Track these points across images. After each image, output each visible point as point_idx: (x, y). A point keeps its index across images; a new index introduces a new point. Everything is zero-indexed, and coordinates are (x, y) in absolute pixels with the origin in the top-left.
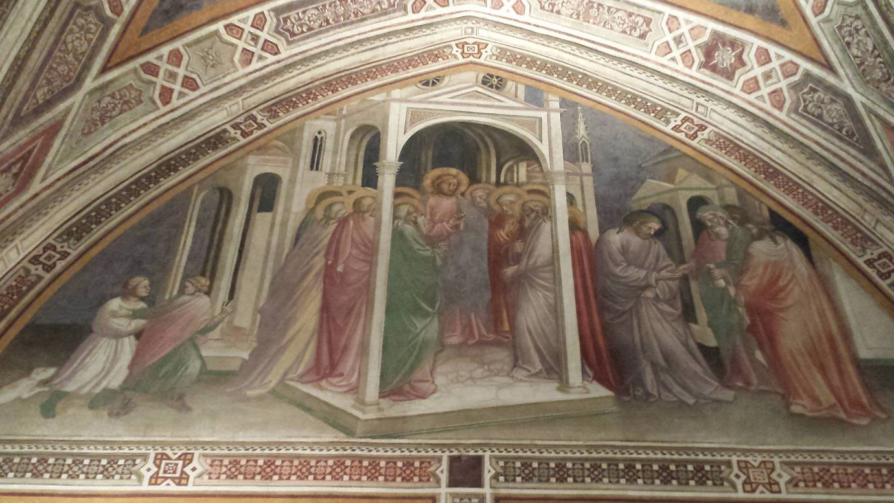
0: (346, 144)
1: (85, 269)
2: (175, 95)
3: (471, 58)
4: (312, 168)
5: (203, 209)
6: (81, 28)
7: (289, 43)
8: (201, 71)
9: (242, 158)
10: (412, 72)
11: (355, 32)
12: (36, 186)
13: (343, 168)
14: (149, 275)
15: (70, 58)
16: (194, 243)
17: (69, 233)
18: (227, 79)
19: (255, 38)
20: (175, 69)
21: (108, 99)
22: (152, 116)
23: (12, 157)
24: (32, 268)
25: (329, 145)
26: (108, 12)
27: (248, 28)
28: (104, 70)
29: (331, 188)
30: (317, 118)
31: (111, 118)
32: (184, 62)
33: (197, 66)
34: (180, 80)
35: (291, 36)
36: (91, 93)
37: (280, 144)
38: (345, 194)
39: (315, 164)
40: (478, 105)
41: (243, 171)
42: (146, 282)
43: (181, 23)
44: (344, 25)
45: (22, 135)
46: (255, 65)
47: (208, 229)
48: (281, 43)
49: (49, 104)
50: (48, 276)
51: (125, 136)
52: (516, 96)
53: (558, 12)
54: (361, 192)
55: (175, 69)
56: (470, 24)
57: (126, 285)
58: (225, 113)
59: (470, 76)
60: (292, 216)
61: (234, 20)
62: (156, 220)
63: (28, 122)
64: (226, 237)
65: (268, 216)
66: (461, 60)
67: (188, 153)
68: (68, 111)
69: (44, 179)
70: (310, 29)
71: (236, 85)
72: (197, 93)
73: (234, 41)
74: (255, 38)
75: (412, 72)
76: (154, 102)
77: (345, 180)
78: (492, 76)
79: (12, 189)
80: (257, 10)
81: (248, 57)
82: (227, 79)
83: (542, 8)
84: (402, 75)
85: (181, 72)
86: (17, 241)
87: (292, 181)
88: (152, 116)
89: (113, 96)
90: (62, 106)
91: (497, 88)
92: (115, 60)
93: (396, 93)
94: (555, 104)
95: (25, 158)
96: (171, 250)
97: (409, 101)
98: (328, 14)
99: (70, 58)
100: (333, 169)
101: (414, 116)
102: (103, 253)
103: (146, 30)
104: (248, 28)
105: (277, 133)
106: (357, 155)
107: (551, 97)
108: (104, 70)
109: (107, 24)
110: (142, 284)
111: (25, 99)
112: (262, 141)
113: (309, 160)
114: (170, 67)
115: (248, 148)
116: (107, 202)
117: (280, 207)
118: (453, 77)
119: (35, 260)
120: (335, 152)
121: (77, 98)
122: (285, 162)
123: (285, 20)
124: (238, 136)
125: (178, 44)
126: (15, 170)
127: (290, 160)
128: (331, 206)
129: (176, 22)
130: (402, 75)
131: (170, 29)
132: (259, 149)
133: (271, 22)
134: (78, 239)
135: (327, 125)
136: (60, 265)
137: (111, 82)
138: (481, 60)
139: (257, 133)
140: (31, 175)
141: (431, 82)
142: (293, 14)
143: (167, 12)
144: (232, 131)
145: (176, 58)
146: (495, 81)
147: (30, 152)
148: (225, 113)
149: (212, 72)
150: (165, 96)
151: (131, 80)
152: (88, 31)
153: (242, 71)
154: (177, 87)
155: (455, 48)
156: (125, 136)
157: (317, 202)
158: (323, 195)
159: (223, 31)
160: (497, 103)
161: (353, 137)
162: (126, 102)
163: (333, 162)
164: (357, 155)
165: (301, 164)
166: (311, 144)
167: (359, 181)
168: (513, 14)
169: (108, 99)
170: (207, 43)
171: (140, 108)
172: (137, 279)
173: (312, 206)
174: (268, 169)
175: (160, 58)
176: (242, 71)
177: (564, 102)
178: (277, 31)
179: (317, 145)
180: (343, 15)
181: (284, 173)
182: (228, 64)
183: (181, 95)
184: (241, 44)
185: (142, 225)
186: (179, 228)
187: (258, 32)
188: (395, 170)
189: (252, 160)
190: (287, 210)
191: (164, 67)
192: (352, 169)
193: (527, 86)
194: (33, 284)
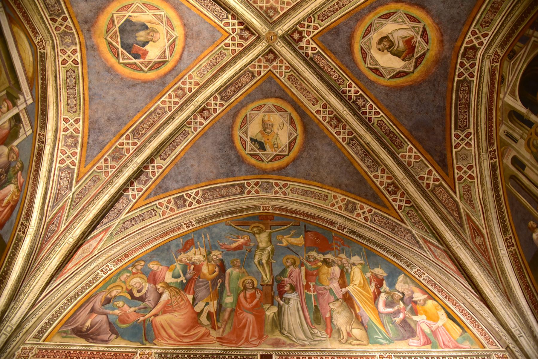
0: (512, 125)
1: (518, 236)
2: (472, 174)
3: (499, 60)
4: (516, 143)
5: (515, 188)
6: (439, 193)
7: (469, 128)
8: (468, 162)
9: (503, 163)
10: (496, 86)
11: (473, 102)
12: (484, 232)
13: (521, 131)
14: (529, 220)
15: (447, 201)
16: (525, 198)
17: (504, 232)
18: (473, 154)
19: (463, 139)
20: (463, 170)
21: (465, 196)
22: (476, 185)
23: (471, 233)
24: (510, 249)
25: (510, 131)
26: (437, 183)
27: (458, 141)
28: (455, 193)
29: (527, 140)
30: (499, 130)
31: (471, 198)
32: (462, 166)
33: (465, 163)
34: (468, 170)
35: (467, 126)
36: (461, 200)
37: (503, 148)
38: (531, 136)
39: (516, 141)
40: (518, 66)
41: (507, 166)
42: (532, 222)
43: (449, 162)
44: (469, 106)
45: (466, 226)
46: (472, 143)
47: (523, 191)
48: (468, 131)
49: (459, 213)
50: (515, 247)
51: (479, 197)
52: (521, 48)
53: (492, 20)
54: (533, 130)
55: (463, 170)
56: (486, 56)
57: (529, 228)
58: (485, 161)
59: (506, 64)
60: (531, 160)
61: (454, 144)
62: (512, 205)
63: (463, 222)
64: (528, 187)
65: (527, 168)
66: (499, 64)
67: (494, 180)
68: (464, 209)
69: (483, 228)
70: (466, 119)
71: (477, 152)
72: (474, 167)
73: (461, 147)
74: (463, 139)
75: (496, 86)
76: (472, 182)
77: (526, 133)
78: (509, 54)
79: (482, 239)
80: (453, 136)
81: (469, 144)
82: (473, 154)
83: (488, 26)
84: (496, 90)
85: (465, 169)
86: (499, 249)
87: (518, 152)
88: (476, 185)
89: (464, 194)
90: (462, 210)
91: (515, 54)
92: (453, 188)
93: (502, 96)
94: (531, 31)
95: (474, 229)
96: (525, 207)
97: (506, 93)
98: (463, 111)
99: (447, 201)
100: (520, 135)
101: (512, 94)
102: (515, 227)
103: (447, 174)
104: (458, 141)
105: (499, 148)
106: (519, 124)
107: (527, 32)
108: (455, 193)
109: (441, 185)
110: (531, 223)
111: (455, 219)
112: (500, 153)
113: (513, 142)
114: (462, 172)
115: (500, 159)
116: (500, 214)
117: (526, 162)
118: (504, 70)
119: (508, 247)
120: (514, 131)
121: (461, 205)
122: (510, 150)
123: (460, 127)
124: (495, 160)
125: (455, 166)
126: (476, 234)
127: (510, 148)
128: (533, 145)
129: (448, 163)
130: (496, 90)
131: (449, 166)
132: (502, 156)
133: (459, 132)
134: (508, 231)
135: (503, 128)
136: (513, 241)
137: (460, 192)
138: (502, 56)
139: (496, 153)
140: (480, 231)
141: (502, 80)
142: (458, 124)
143: (444, 165)
144: (492, 161)
145: (460, 169)
146: (511, 54)
147: (473, 227)
148: (485, 161)
149: (469, 159)
150: (471, 177)
151: (461, 186)
152: (441, 192)
153: (473, 148)
154: (470, 172)
155: (493, 64)
156: (479, 197)
157: (530, 148)
158: (528, 144)
159: (456, 150)
160: (521, 57)
161: (511, 121)
162: (468, 191)
163: (517, 133)
164: (519, 124)
165: (513, 145)
166: (507, 137)
167: (529, 129)
168: (487, 38)
169: (465, 196)
170: (459, 157)
171: (472, 188)
172: (529, 223)
173: (530, 151)
174: (510, 158)
175: (458, 174)
176: (473, 148)
177: (531, 27)
178: (463, 131)
179: (508, 135)
180: (465, 105)
181: (514, 153)
182: (468, 152)
183: (473, 172)
184: (463, 145)
185: (512, 210)
186: (518, 200)
187: (461, 138)
188: (530, 113)
189: (505, 161)
190: (528, 161)
191: (461, 173)
192: (523, 129)
193: (519, 41)
194: (516, 253)
